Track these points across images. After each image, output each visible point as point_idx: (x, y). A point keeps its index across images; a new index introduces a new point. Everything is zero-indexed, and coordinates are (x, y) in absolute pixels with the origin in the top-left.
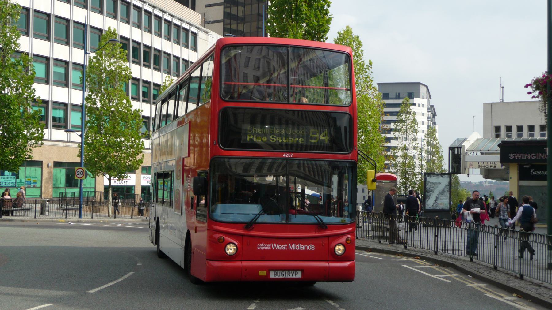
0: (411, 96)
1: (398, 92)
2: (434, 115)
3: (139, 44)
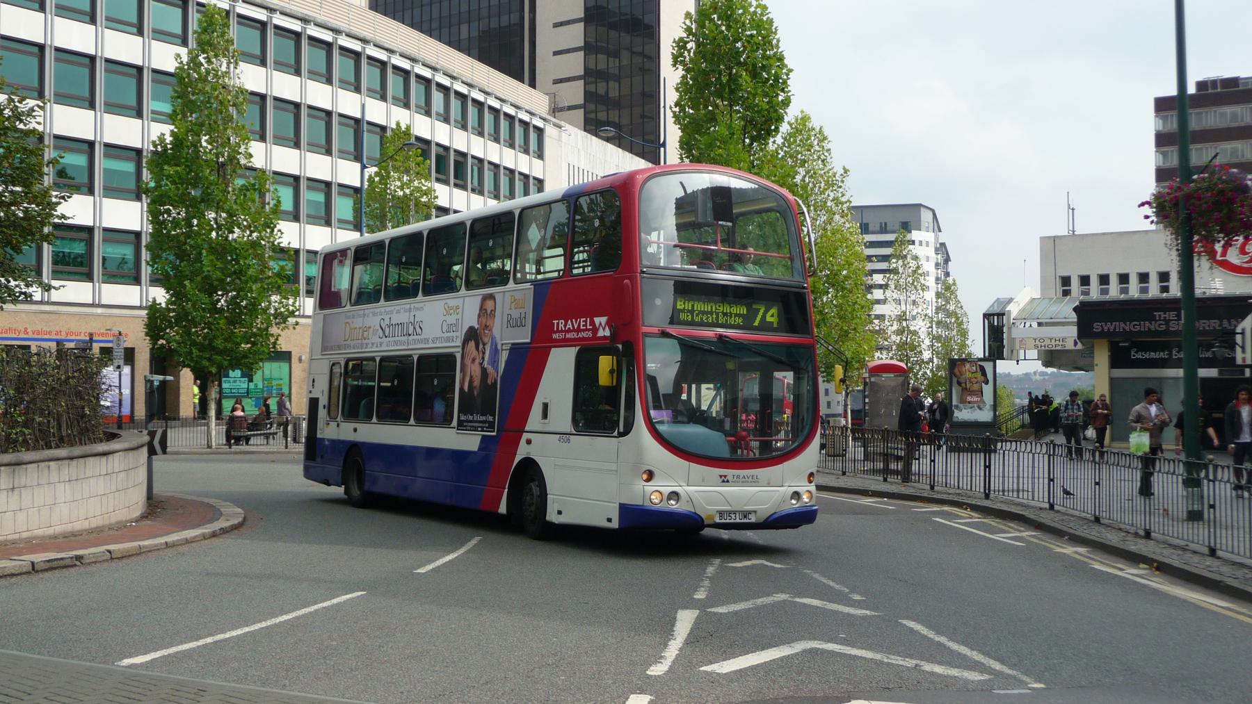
0: (906, 227)
2: (947, 260)
3: (446, 149)
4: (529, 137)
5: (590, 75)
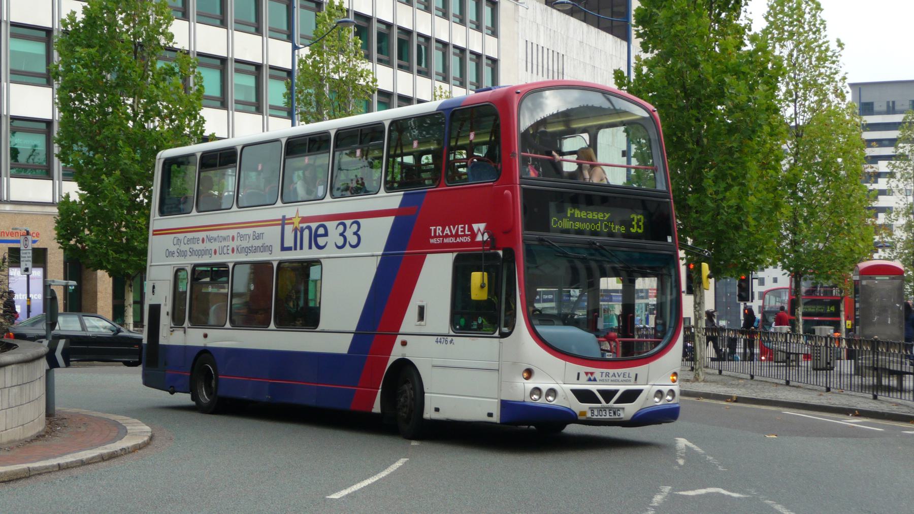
1: (891, 100)
3: (389, 26)
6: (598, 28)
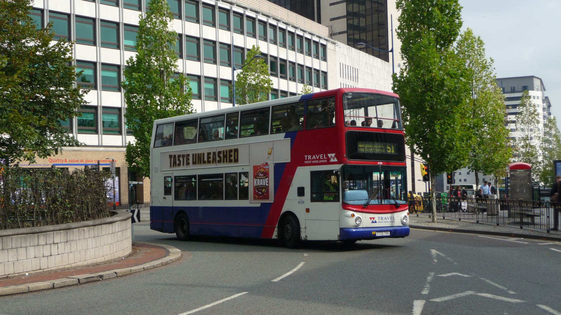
0: (525, 89)
2: (549, 106)
3: (276, 58)
4: (320, 51)
5: (350, 15)
6: (373, 55)
